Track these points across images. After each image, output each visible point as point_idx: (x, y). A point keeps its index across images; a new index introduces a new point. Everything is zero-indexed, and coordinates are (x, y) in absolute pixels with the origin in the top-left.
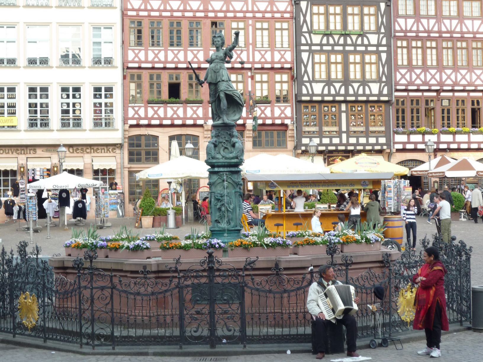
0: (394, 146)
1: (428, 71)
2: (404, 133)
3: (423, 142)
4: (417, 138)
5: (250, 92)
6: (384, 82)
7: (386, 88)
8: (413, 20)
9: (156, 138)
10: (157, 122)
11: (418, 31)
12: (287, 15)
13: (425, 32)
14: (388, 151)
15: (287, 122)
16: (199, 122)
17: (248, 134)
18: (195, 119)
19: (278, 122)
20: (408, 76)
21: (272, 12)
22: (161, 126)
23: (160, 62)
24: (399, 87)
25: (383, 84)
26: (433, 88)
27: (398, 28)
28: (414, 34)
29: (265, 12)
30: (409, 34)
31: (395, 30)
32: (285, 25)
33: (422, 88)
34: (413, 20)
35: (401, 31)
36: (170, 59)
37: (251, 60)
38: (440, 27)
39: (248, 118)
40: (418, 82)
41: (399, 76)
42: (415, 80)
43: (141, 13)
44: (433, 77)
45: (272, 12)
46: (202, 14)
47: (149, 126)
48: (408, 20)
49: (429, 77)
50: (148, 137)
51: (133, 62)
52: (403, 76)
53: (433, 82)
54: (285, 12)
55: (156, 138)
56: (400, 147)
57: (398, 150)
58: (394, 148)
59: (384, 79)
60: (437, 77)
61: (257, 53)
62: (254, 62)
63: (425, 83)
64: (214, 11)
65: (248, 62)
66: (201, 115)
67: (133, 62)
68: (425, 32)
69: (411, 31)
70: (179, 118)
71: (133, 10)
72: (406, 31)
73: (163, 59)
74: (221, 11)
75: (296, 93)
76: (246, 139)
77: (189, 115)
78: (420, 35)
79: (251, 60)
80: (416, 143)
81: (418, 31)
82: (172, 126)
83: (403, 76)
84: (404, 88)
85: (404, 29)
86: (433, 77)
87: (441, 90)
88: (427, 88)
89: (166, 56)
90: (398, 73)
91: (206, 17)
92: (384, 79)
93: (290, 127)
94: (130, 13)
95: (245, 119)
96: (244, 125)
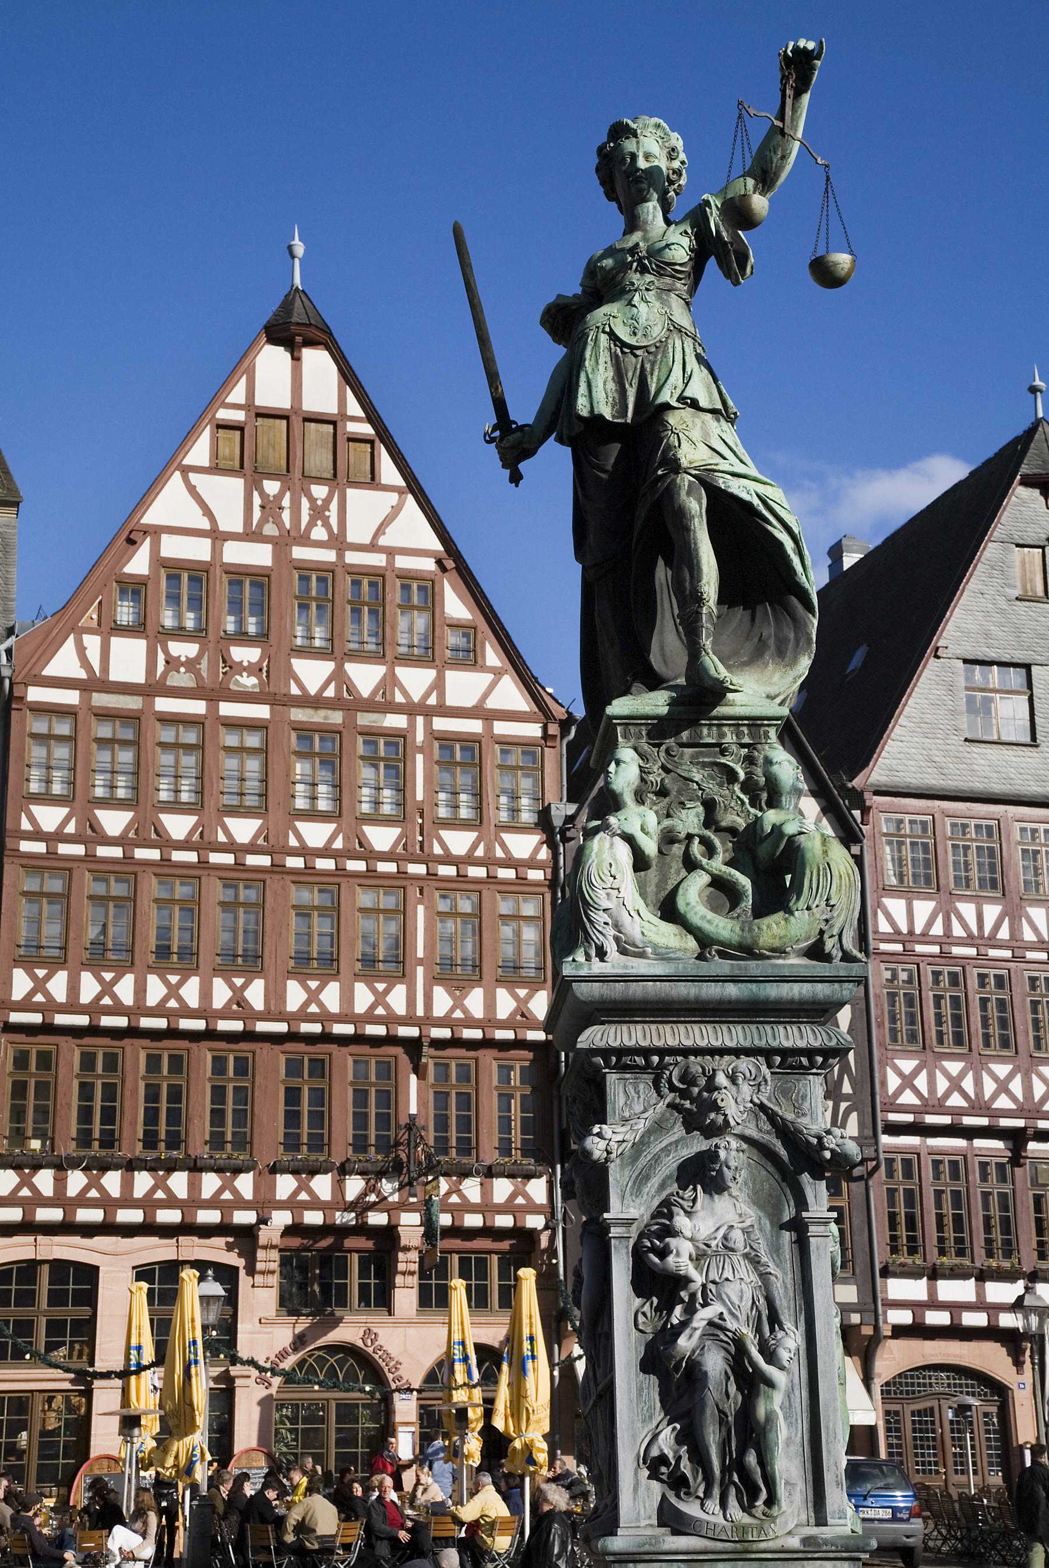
0: (885, 1313)
1: (983, 1066)
2: (914, 1274)
3: (980, 1305)
4: (960, 1290)
5: (412, 1118)
6: (847, 1098)
7: (854, 1117)
8: (932, 904)
9: (89, 1274)
10: (95, 1215)
11: (947, 939)
12: (536, 875)
13: (970, 940)
14: (867, 1331)
15: (535, 1222)
16: (244, 1217)
17: (408, 1261)
18: (227, 1208)
19: (505, 1221)
20: (921, 1082)
21: (488, 862)
22: (108, 1228)
23: (118, 1009)
24: (893, 1117)
25: (843, 1105)
26: (1004, 1122)
27: (884, 927)
28: (935, 949)
29: (470, 859)
30: (920, 948)
31: (876, 932)
32: (529, 909)
33: (968, 1121)
34: (932, 904)
35: (896, 936)
36: (152, 999)
37: (420, 1012)
38: (1015, 931)
39: (404, 1206)
40: (956, 1100)
41: (893, 1082)
42: (947, 1094)
43: (64, 849)
44: (1003, 1087)
45: (488, 862)
46: (265, 861)
47: (67, 1228)
48: (917, 904)
49: (989, 1087)
50: (59, 1267)
51: (25, 1005)
52: (908, 1082)
53: (1003, 1102)
54: (532, 863)
55: (89, 1274)
56: (904, 1317)
57: (899, 1332)
58: (885, 1322)
59: (847, 1088)
60: (1016, 1086)
61: (439, 992)
62: (429, 1020)
63: (979, 1106)
64: (304, 851)
65: (409, 1020)
66: (247, 1193)
67: (25, 1005)
68: (970, 940)
69: (925, 938)
70: (171, 1202)
71: (37, 835)
72: (909, 938)
73: (128, 1000)
74: (326, 852)
75: (565, 1126)
76: (399, 1280)
77: (207, 1193)
78: (957, 951)
79: (420, 1012)
80: (955, 1308)
81: (947, 939)
82: (148, 1229)
83: (908, 1082)
84: (909, 1118)
85: (904, 929)
86: (1003, 1087)
87: (1030, 1131)
88: (984, 1121)
89: (140, 990)
90: (890, 1073)
91: (277, 868)
92: (847, 1088)
93: (544, 1243)
94: (26, 846)
95: (392, 1210)
96: (389, 1235)
